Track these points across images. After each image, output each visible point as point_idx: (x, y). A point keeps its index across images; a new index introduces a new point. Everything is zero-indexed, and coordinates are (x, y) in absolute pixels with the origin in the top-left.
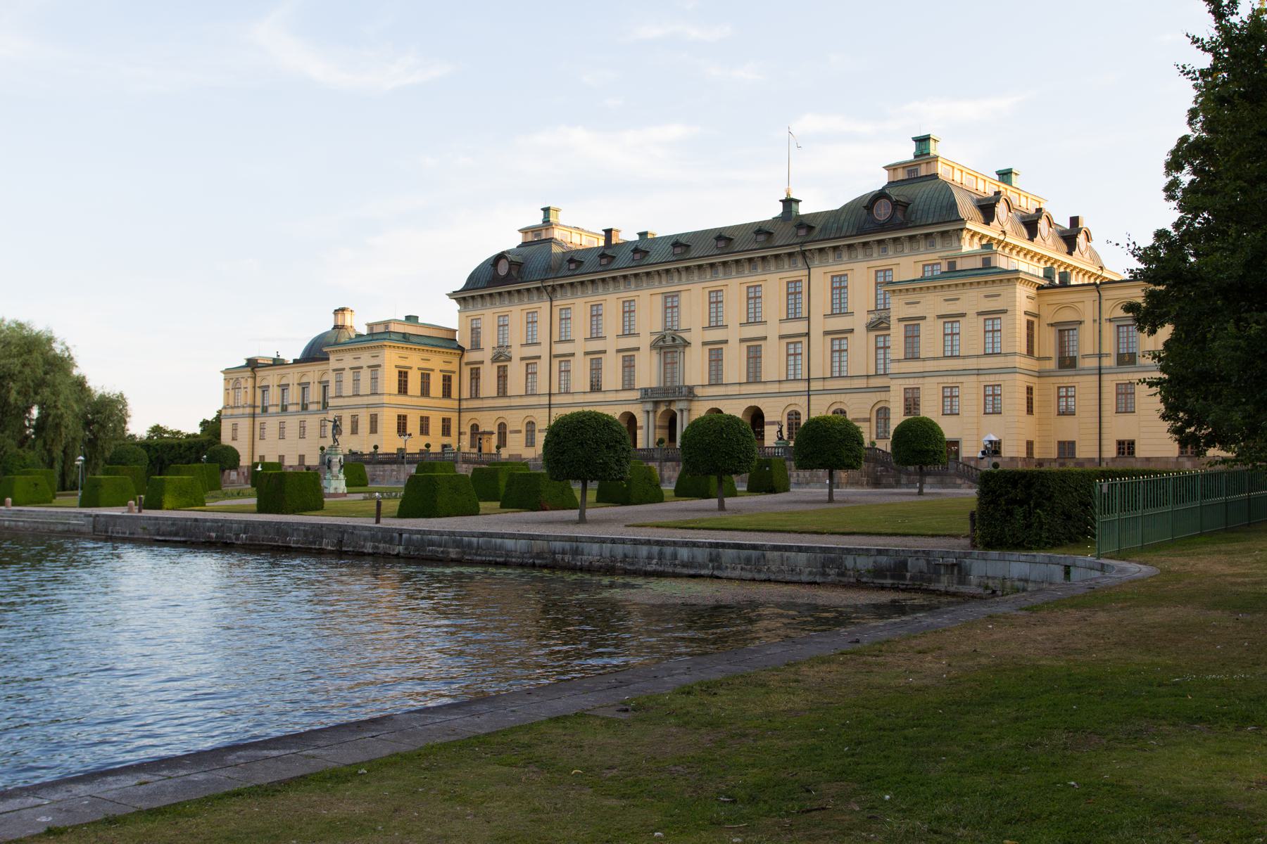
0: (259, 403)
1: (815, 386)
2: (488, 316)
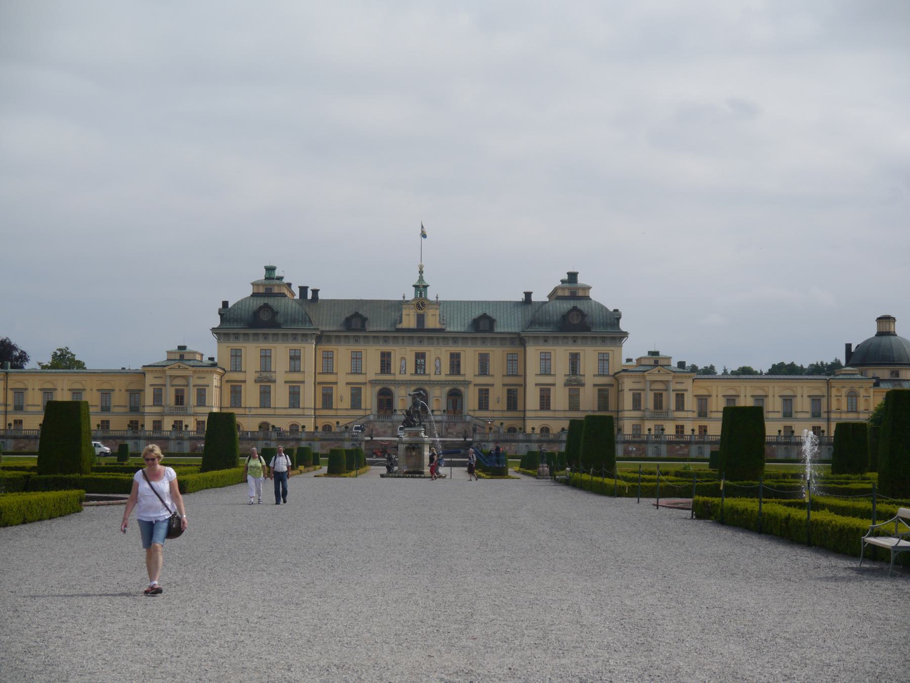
0: (10, 401)
1: (528, 414)
2: (251, 351)
